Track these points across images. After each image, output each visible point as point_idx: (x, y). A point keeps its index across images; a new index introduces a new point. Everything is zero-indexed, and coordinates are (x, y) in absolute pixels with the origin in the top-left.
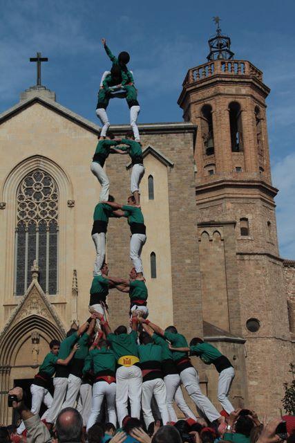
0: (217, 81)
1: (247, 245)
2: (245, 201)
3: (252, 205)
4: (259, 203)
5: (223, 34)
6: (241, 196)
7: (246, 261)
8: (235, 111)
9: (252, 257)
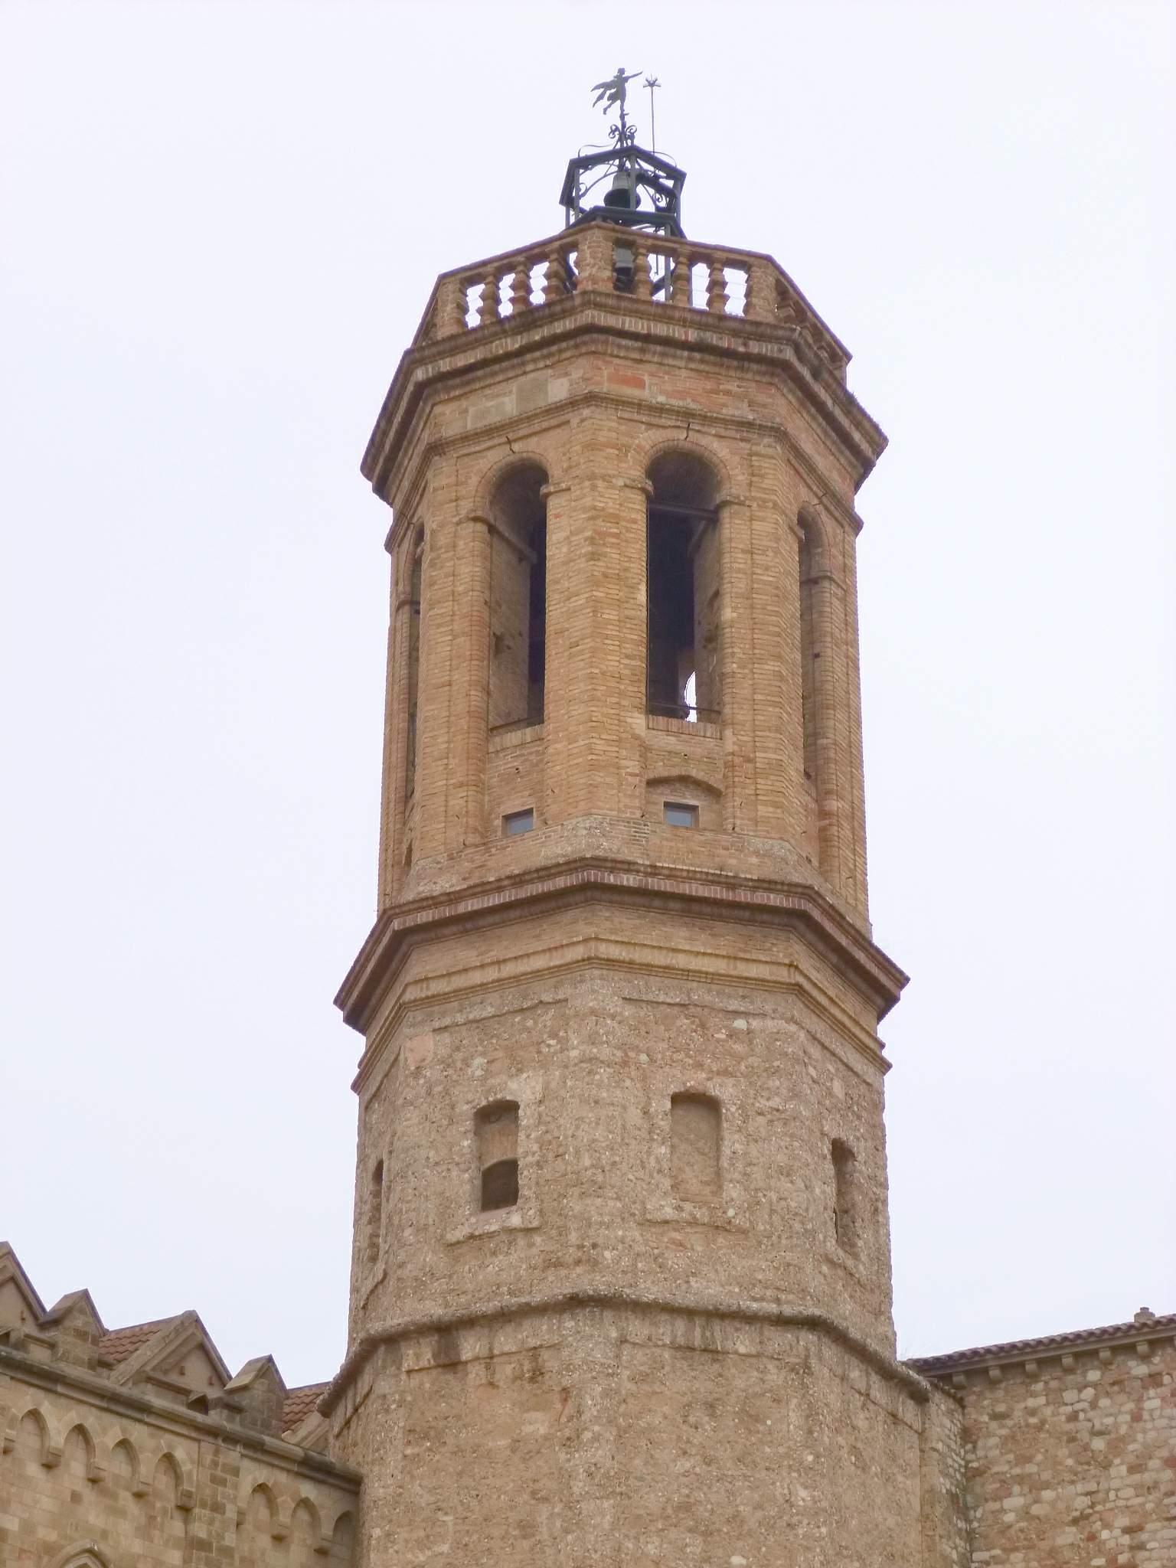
0: (421, 387)
1: (494, 1265)
2: (511, 999)
3: (548, 1017)
4: (599, 994)
5: (642, 142)
6: (491, 974)
7: (476, 1374)
8: (680, 515)
9: (506, 1340)
